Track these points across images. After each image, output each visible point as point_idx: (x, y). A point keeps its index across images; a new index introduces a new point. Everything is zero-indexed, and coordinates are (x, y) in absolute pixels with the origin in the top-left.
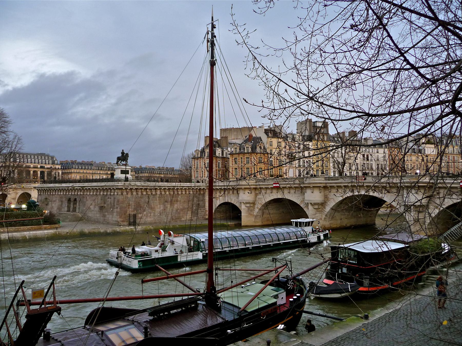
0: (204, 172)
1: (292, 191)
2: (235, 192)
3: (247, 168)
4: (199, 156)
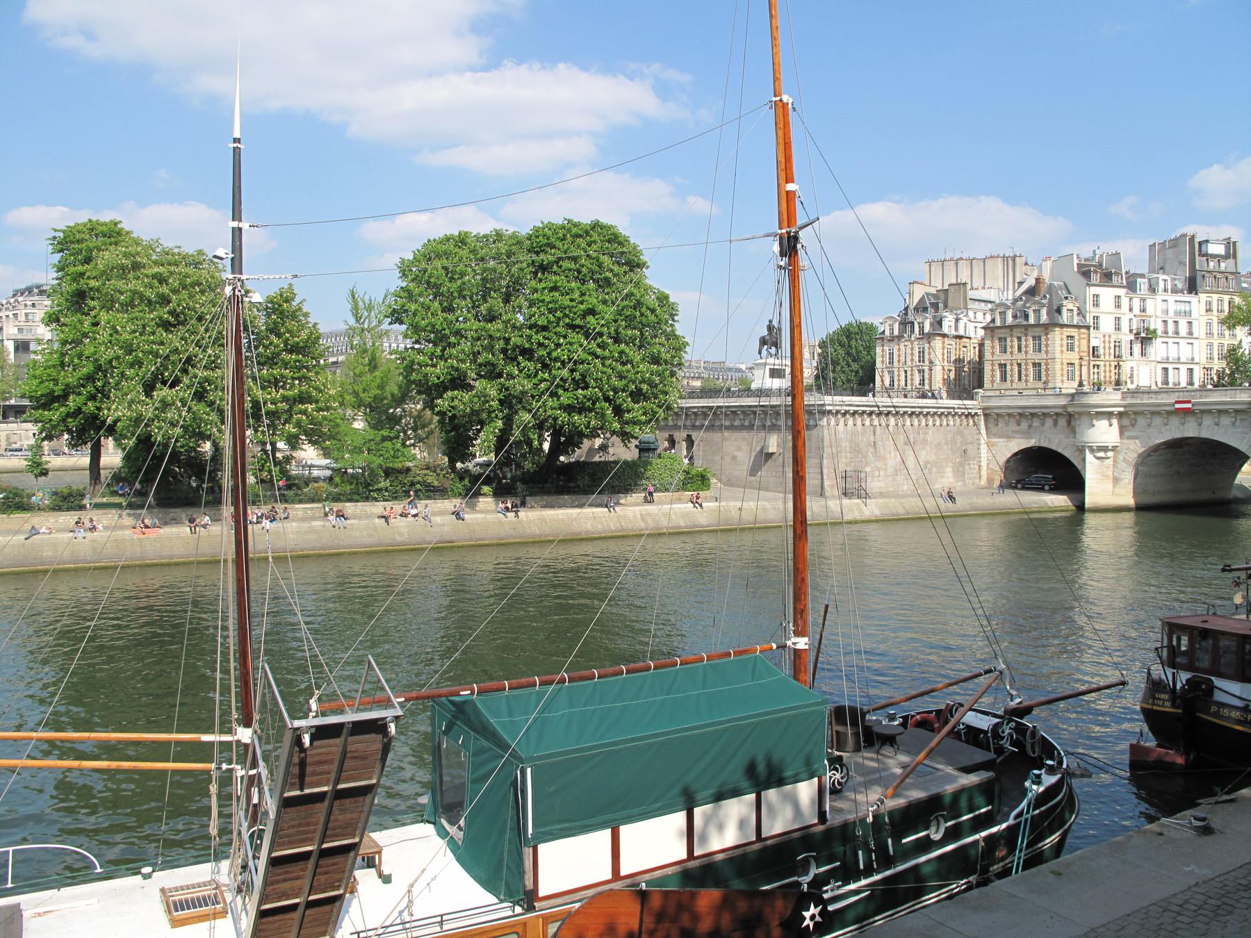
0: (909, 373)
1: (1226, 421)
2: (1062, 422)
3: (1034, 365)
4: (896, 333)
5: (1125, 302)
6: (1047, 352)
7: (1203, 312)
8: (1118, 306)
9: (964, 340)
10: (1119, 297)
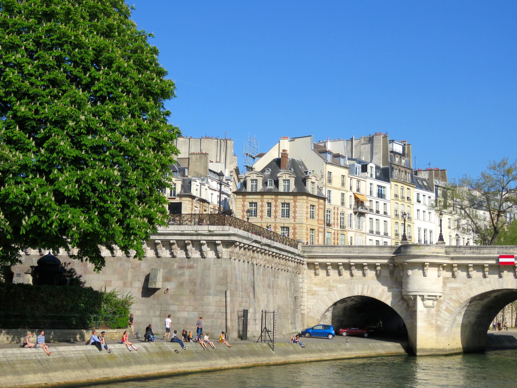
5: (347, 180)
6: (295, 218)
7: (393, 197)
8: (343, 184)
9: (206, 204)
10: (343, 176)
